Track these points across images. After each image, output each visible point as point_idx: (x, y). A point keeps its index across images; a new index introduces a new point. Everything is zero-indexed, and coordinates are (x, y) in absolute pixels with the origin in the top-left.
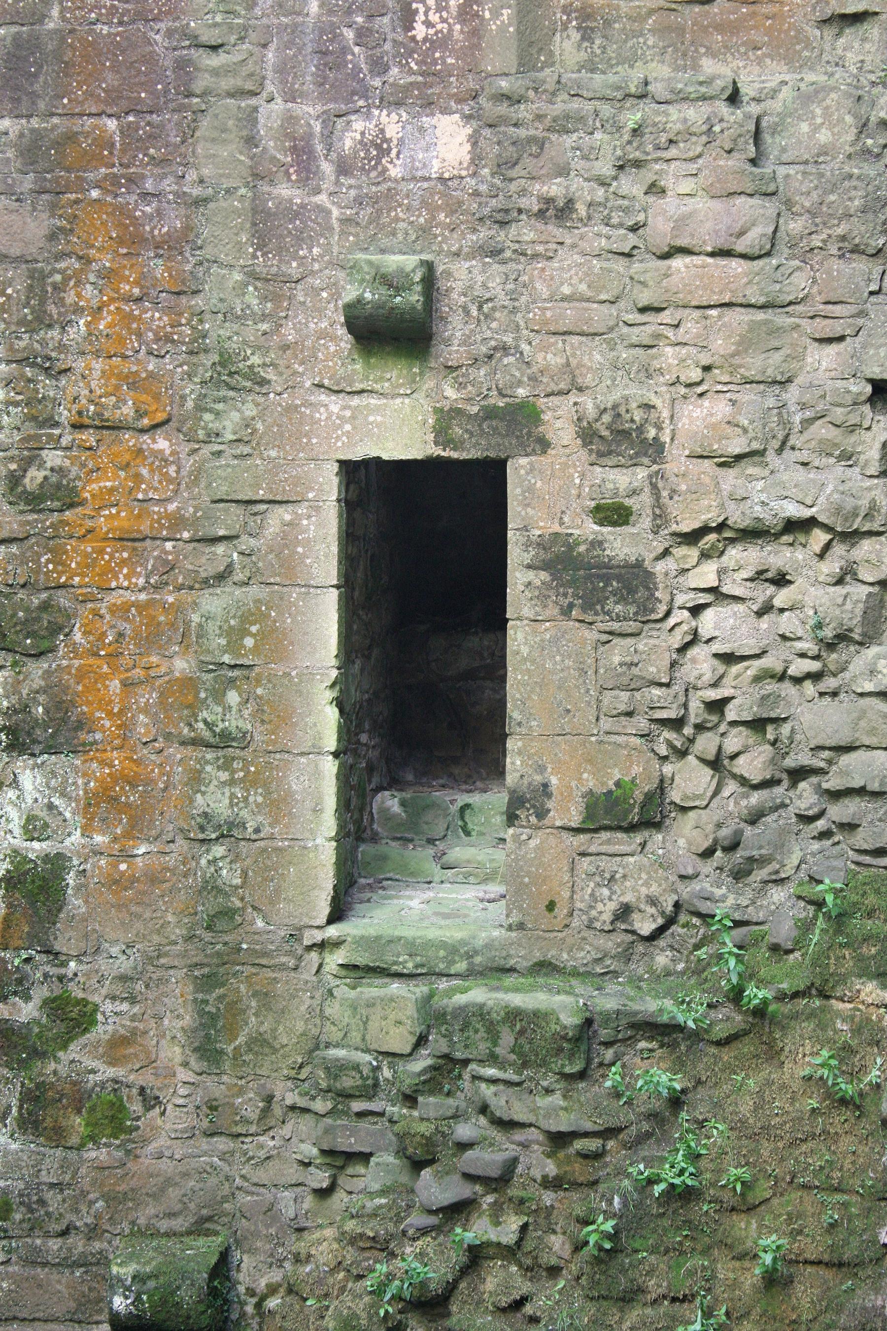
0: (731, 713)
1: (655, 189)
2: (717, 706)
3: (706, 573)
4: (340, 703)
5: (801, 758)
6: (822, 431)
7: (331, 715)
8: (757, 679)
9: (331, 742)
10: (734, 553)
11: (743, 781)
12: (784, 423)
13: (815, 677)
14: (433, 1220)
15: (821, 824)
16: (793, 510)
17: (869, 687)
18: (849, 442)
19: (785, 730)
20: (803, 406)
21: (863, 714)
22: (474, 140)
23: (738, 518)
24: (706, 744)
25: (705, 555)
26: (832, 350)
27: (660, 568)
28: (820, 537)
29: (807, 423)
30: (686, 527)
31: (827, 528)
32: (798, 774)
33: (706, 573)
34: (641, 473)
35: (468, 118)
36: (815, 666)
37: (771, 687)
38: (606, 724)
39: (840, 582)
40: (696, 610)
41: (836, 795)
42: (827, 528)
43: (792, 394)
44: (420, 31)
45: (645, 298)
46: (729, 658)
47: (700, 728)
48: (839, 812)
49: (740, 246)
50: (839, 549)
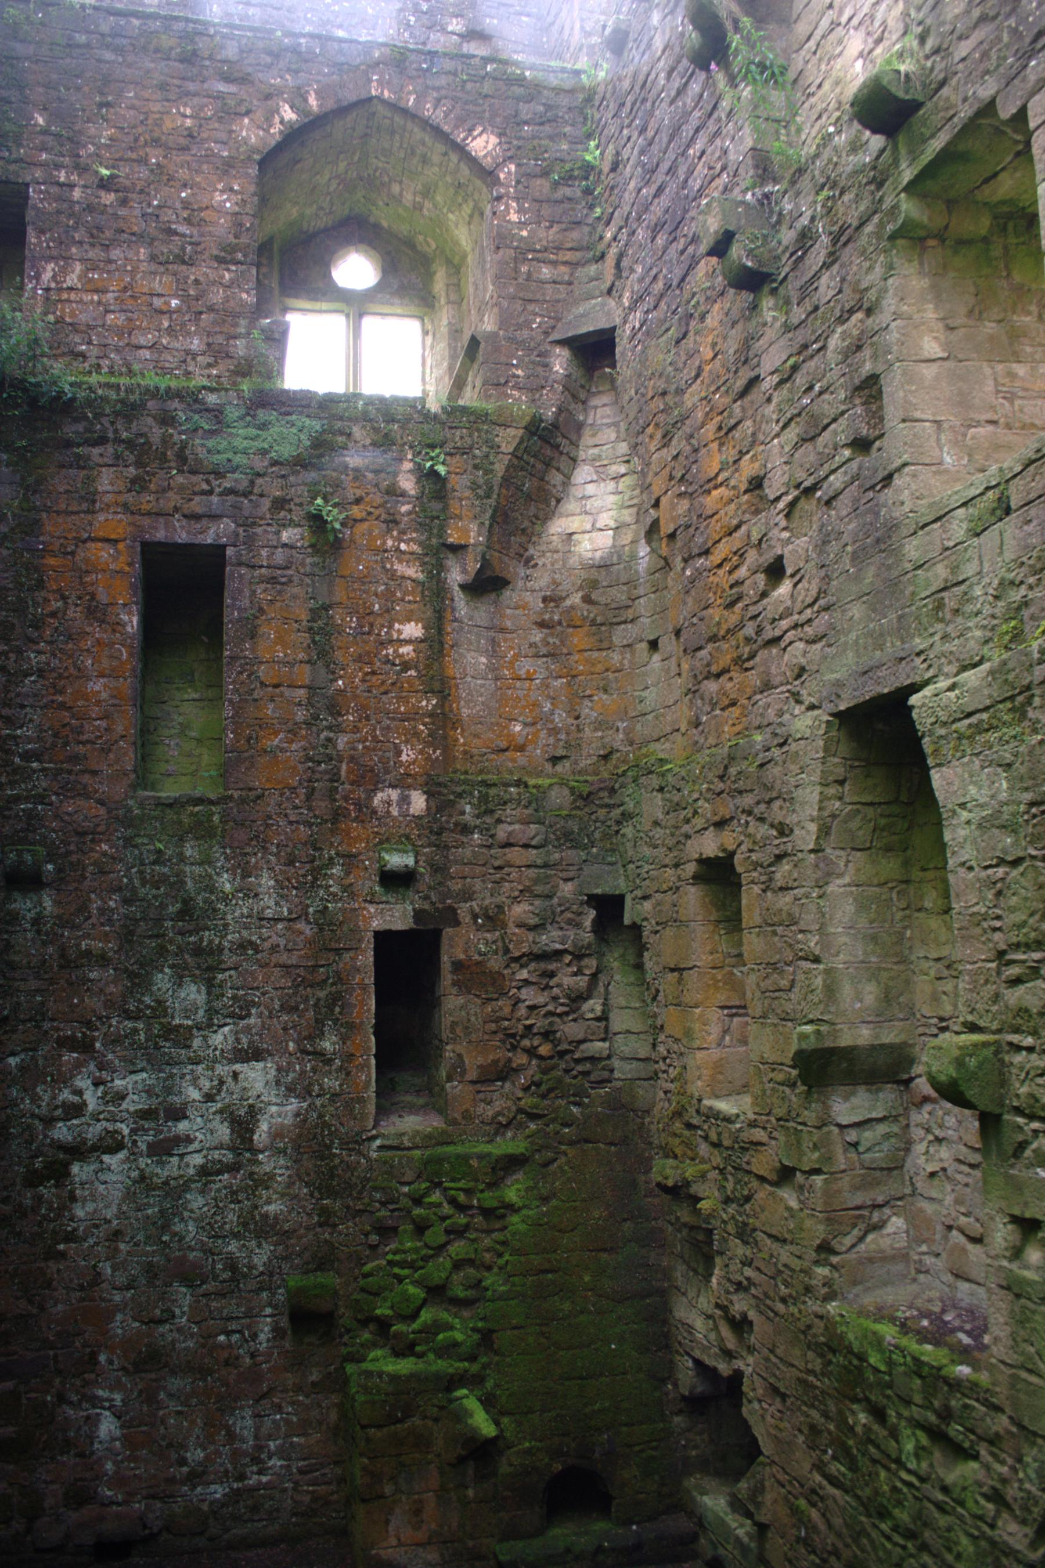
0: (535, 1030)
1: (499, 821)
2: (529, 1028)
3: (524, 974)
4: (375, 1034)
5: (564, 1046)
6: (568, 915)
7: (373, 1038)
8: (545, 1016)
9: (374, 1051)
10: (533, 966)
11: (541, 1058)
12: (553, 913)
13: (567, 1014)
14: (431, 1252)
15: (574, 1073)
16: (558, 946)
17: (590, 1015)
18: (578, 919)
19: (558, 1035)
20: (560, 905)
21: (589, 1027)
22: (427, 801)
23: (536, 950)
24: (526, 1043)
25: (522, 966)
26: (570, 884)
27: (506, 972)
28: (568, 958)
29: (562, 912)
30: (517, 954)
31: (570, 953)
32: (562, 1054)
33: (524, 974)
34: (497, 933)
35: (425, 793)
36: (566, 1009)
37: (551, 1019)
38: (486, 1037)
39: (575, 974)
40: (519, 988)
41: (578, 1061)
42: (570, 953)
43: (555, 900)
44: (404, 758)
45: (497, 863)
46: (532, 1008)
47: (523, 1037)
48: (580, 1068)
49: (534, 843)
50: (575, 962)
